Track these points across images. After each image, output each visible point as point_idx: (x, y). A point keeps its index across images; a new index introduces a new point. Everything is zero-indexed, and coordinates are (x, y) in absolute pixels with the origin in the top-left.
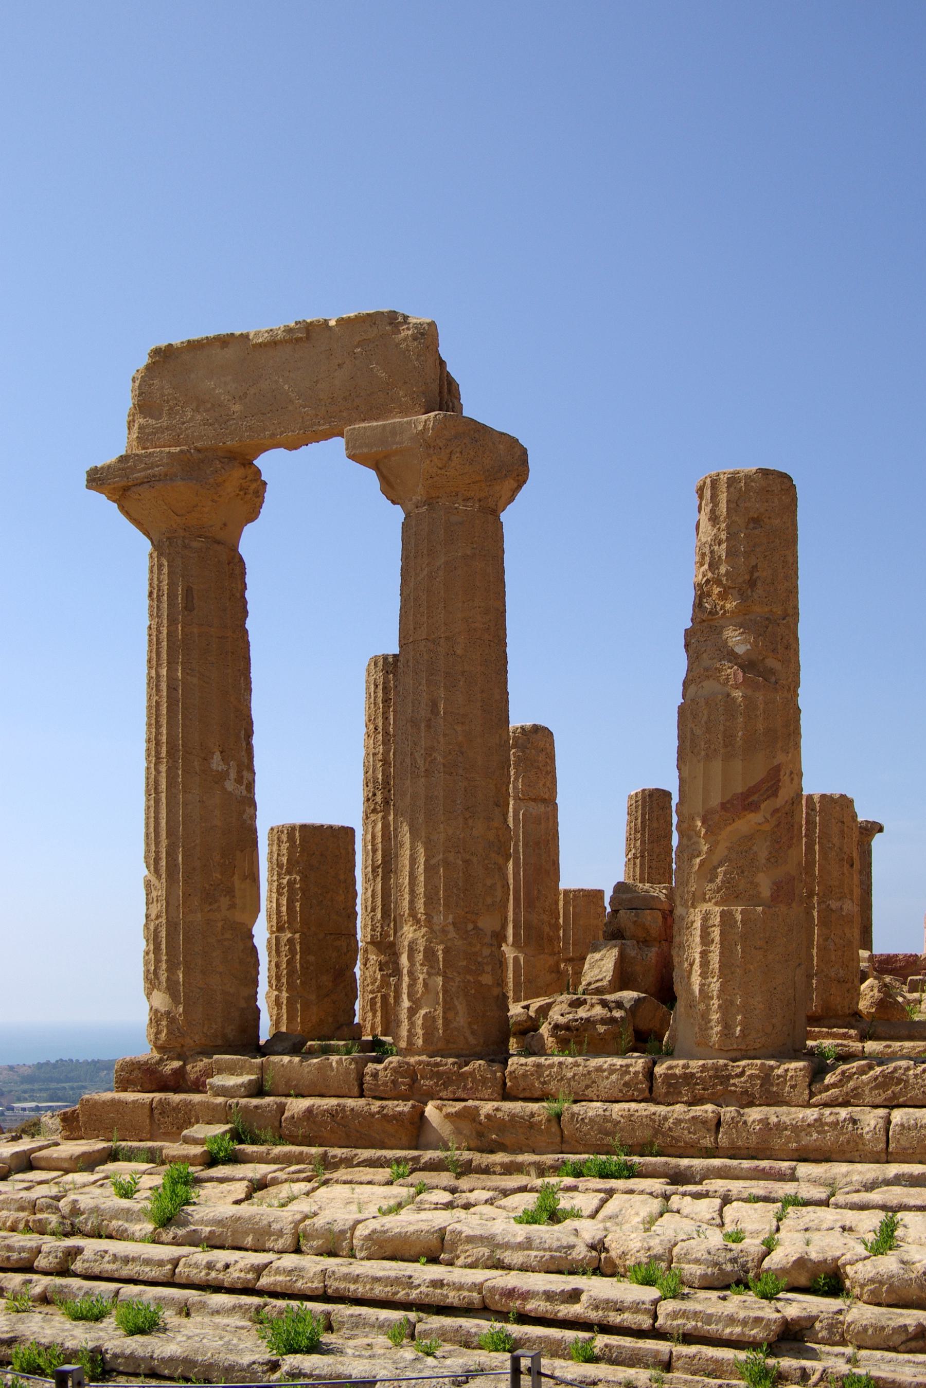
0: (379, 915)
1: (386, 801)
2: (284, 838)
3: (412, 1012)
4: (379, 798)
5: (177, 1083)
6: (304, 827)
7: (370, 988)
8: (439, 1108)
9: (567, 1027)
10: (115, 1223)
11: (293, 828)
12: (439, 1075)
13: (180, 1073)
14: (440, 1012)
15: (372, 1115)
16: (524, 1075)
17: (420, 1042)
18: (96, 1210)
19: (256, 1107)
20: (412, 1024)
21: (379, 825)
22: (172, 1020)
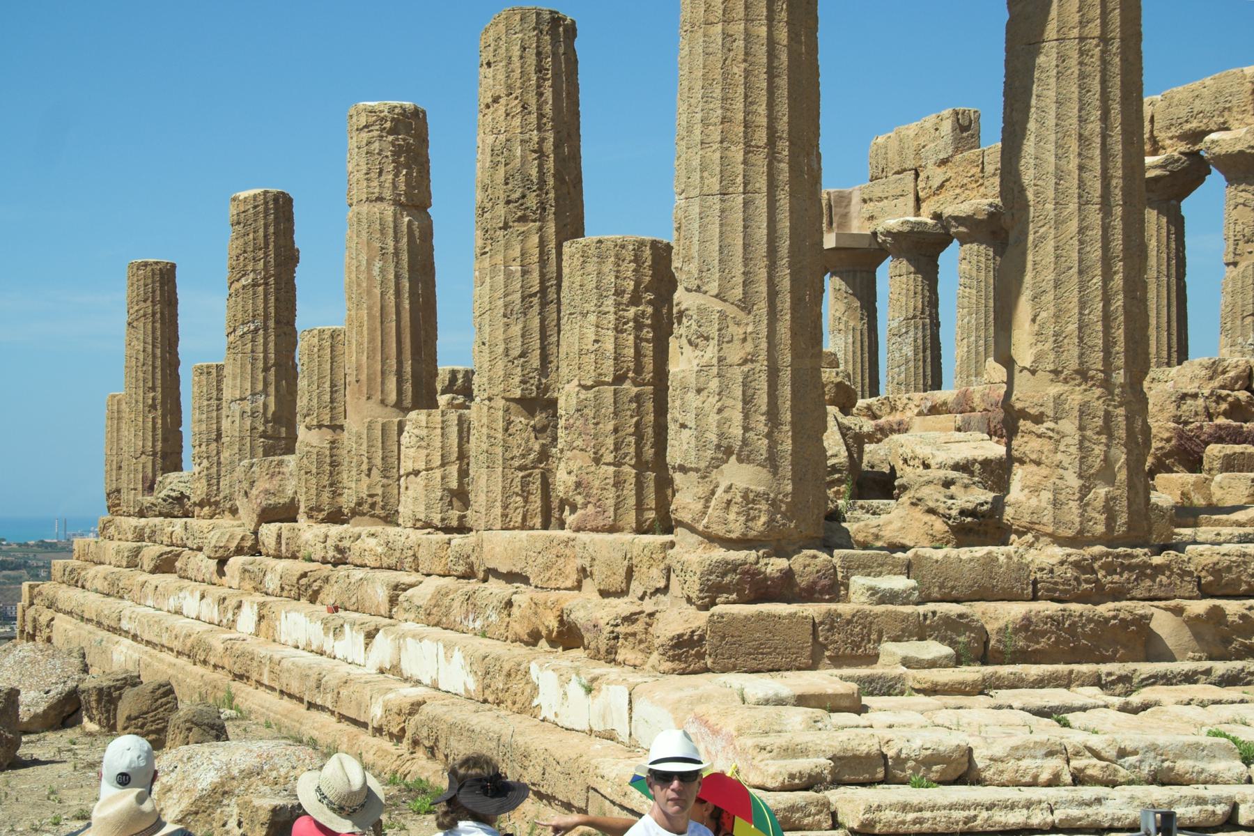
0: (535, 362)
1: (543, 207)
2: (628, 254)
3: (1085, 490)
4: (532, 201)
5: (784, 589)
6: (654, 244)
7: (516, 463)
8: (1178, 611)
9: (972, 513)
10: (1182, 766)
11: (642, 243)
12: (1130, 568)
13: (788, 574)
14: (1122, 492)
15: (1107, 620)
16: (1229, 569)
17: (1100, 529)
18: (1153, 748)
19: (961, 616)
20: (1084, 506)
21: (535, 239)
22: (774, 504)
